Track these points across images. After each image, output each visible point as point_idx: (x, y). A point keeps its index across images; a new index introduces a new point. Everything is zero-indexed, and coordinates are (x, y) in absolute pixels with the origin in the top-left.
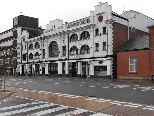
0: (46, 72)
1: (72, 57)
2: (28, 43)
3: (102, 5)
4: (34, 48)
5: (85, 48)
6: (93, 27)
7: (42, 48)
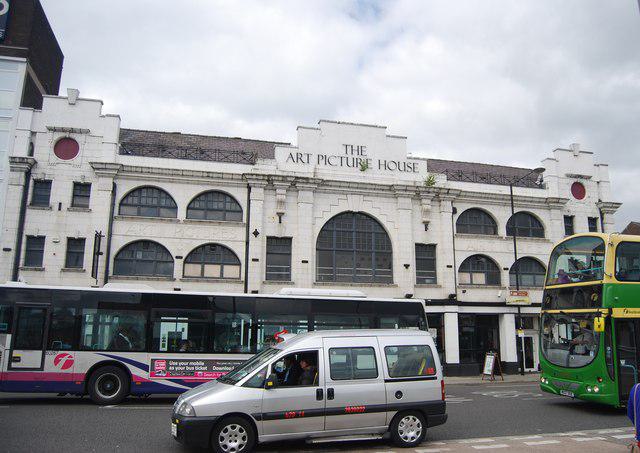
2: (116, 177)
3: (80, 102)
4: (182, 213)
6: (560, 208)
7: (263, 228)
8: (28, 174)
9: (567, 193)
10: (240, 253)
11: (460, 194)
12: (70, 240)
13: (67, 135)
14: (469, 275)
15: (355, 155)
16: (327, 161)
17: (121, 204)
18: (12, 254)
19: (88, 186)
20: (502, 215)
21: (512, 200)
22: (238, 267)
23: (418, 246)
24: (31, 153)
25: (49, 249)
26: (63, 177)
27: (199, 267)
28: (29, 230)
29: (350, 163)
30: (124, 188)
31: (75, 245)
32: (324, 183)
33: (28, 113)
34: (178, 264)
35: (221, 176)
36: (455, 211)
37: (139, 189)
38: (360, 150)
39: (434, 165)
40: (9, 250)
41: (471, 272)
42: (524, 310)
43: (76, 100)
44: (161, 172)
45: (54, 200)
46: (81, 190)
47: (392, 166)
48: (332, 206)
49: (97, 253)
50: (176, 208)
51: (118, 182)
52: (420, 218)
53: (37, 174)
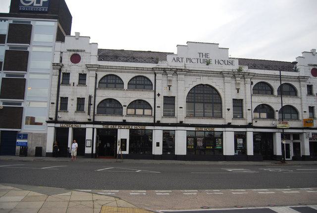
0: (181, 148)
1: (260, 123)
2: (97, 71)
4: (126, 86)
5: (289, 111)
6: (305, 81)
8: (60, 70)
9: (309, 74)
10: (152, 103)
11: (254, 75)
12: (78, 98)
13: (76, 53)
14: (258, 113)
15: (204, 58)
16: (191, 61)
17: (99, 83)
18: (55, 105)
19: (85, 75)
20: (276, 85)
21: (280, 78)
22: (151, 110)
23: (233, 99)
24: (61, 61)
25: (70, 102)
26: (74, 71)
27: (134, 110)
28: (61, 95)
29: (202, 62)
30: (101, 75)
31: (80, 101)
32: (189, 71)
33: (59, 44)
34: (125, 109)
35: (143, 69)
36: (252, 83)
37: (107, 76)
38: (206, 55)
39: (242, 61)
40: (54, 103)
41: (260, 113)
42: (286, 131)
43: (78, 37)
44: (116, 68)
45: (71, 81)
46: (82, 78)
47: (221, 62)
48: (192, 82)
49: (90, 104)
50: (123, 84)
51: (98, 73)
52: (234, 87)
53: (64, 70)
